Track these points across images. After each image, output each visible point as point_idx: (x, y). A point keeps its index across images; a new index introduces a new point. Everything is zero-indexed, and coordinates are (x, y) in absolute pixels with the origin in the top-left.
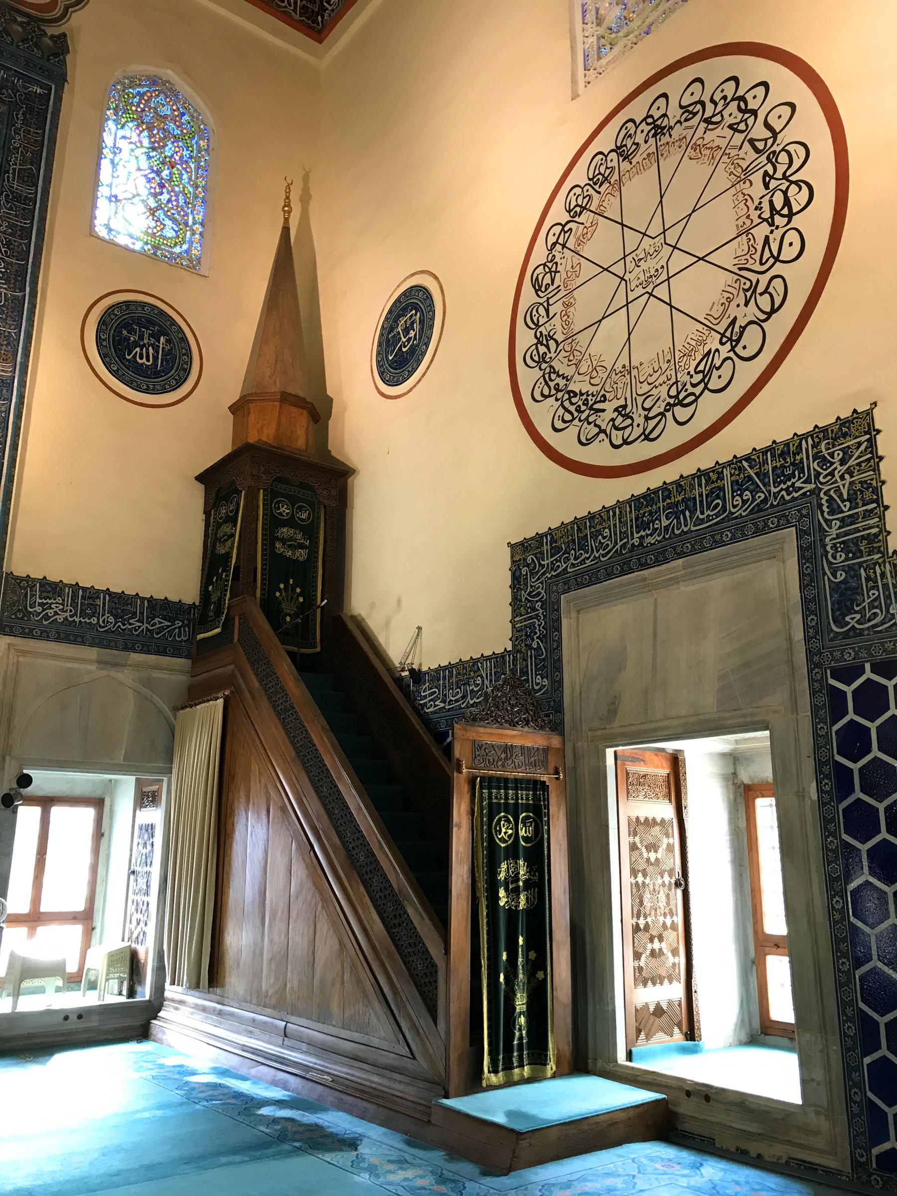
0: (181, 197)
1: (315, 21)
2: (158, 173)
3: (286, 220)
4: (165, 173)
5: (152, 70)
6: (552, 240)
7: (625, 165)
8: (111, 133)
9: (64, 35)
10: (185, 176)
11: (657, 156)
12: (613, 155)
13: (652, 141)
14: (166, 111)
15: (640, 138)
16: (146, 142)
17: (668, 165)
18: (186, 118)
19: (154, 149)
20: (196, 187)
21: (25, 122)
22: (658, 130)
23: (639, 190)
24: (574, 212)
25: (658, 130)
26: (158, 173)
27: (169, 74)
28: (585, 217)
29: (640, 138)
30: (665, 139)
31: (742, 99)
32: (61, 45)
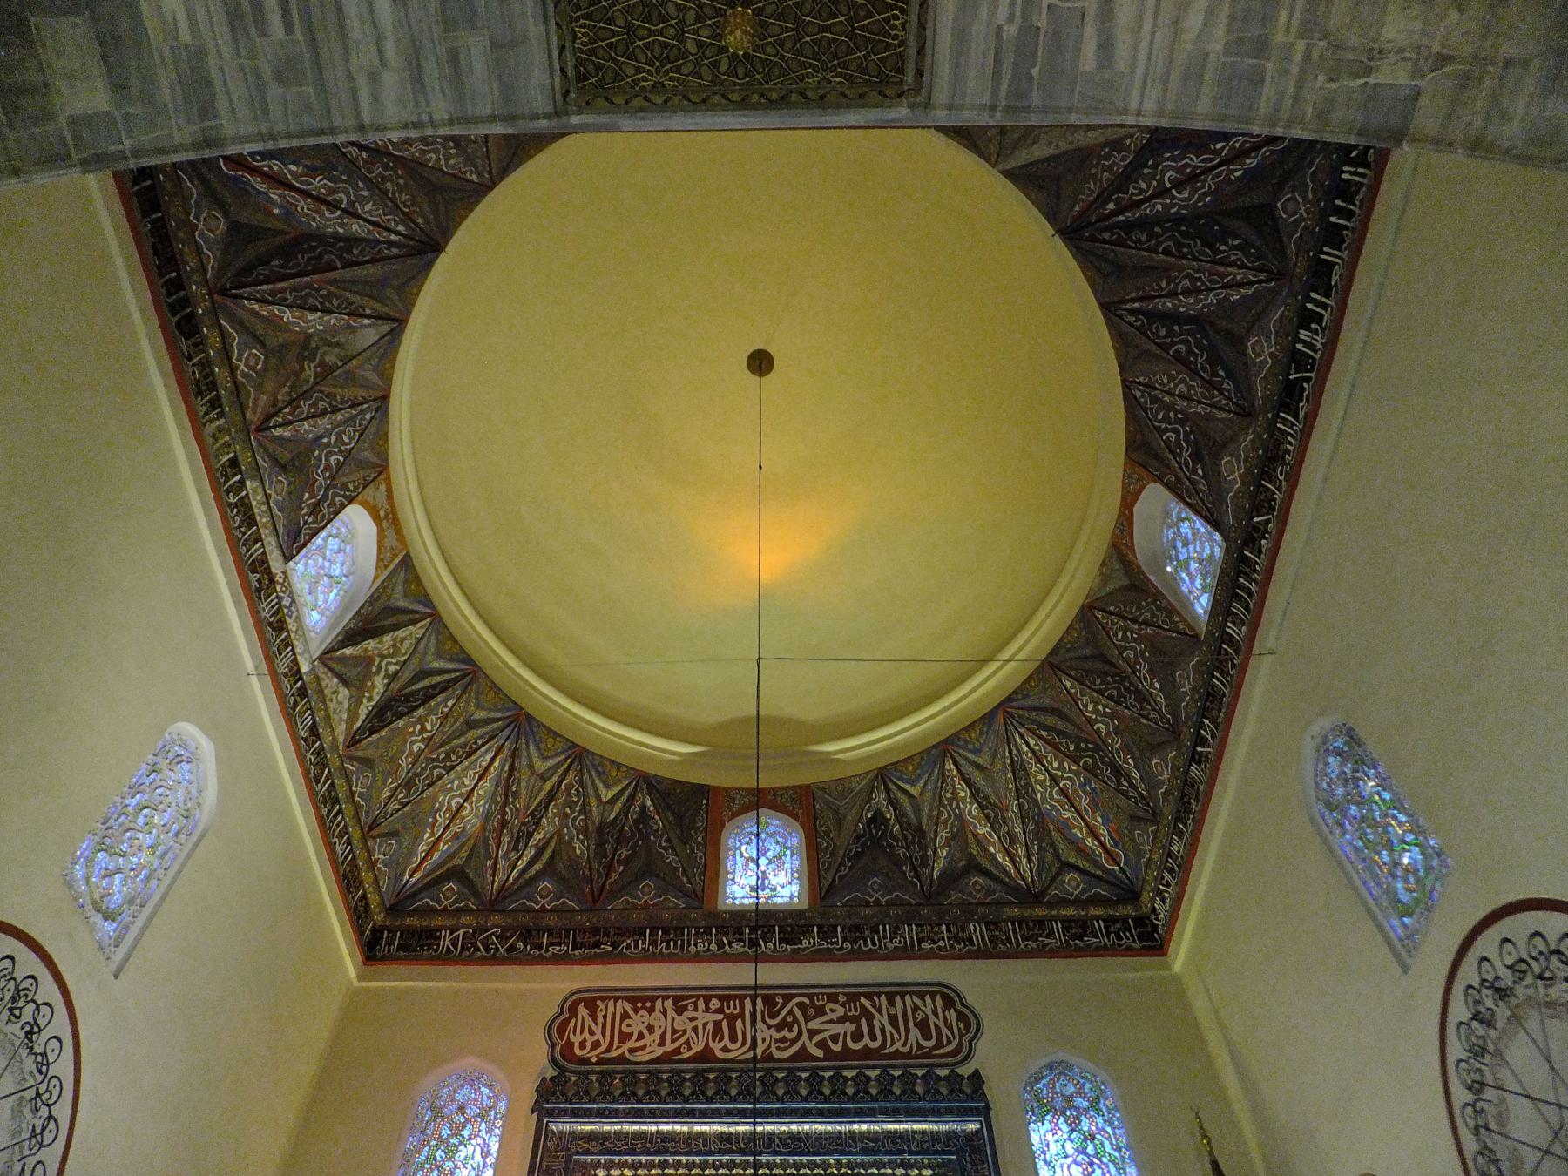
0: (1111, 1166)
1: (1154, 940)
2: (1084, 1152)
3: (1211, 1153)
4: (1090, 1149)
5: (1046, 1061)
6: (1471, 1123)
7: (1493, 1033)
8: (1039, 1133)
9: (977, 1071)
10: (1107, 1143)
11: (1515, 1018)
12: (1475, 1024)
13: (1501, 1003)
14: (1071, 1089)
15: (1489, 1003)
16: (1065, 1128)
17: (1533, 1024)
18: (1088, 1086)
19: (1073, 1130)
20: (1119, 1149)
21: (973, 1163)
22: (1503, 993)
23: (1521, 1056)
24: (1477, 1087)
25: (1503, 993)
26: (1084, 1152)
27: (1061, 1056)
28: (1489, 1094)
29: (1489, 1003)
30: (1514, 1001)
31: (1558, 952)
32: (976, 1078)
